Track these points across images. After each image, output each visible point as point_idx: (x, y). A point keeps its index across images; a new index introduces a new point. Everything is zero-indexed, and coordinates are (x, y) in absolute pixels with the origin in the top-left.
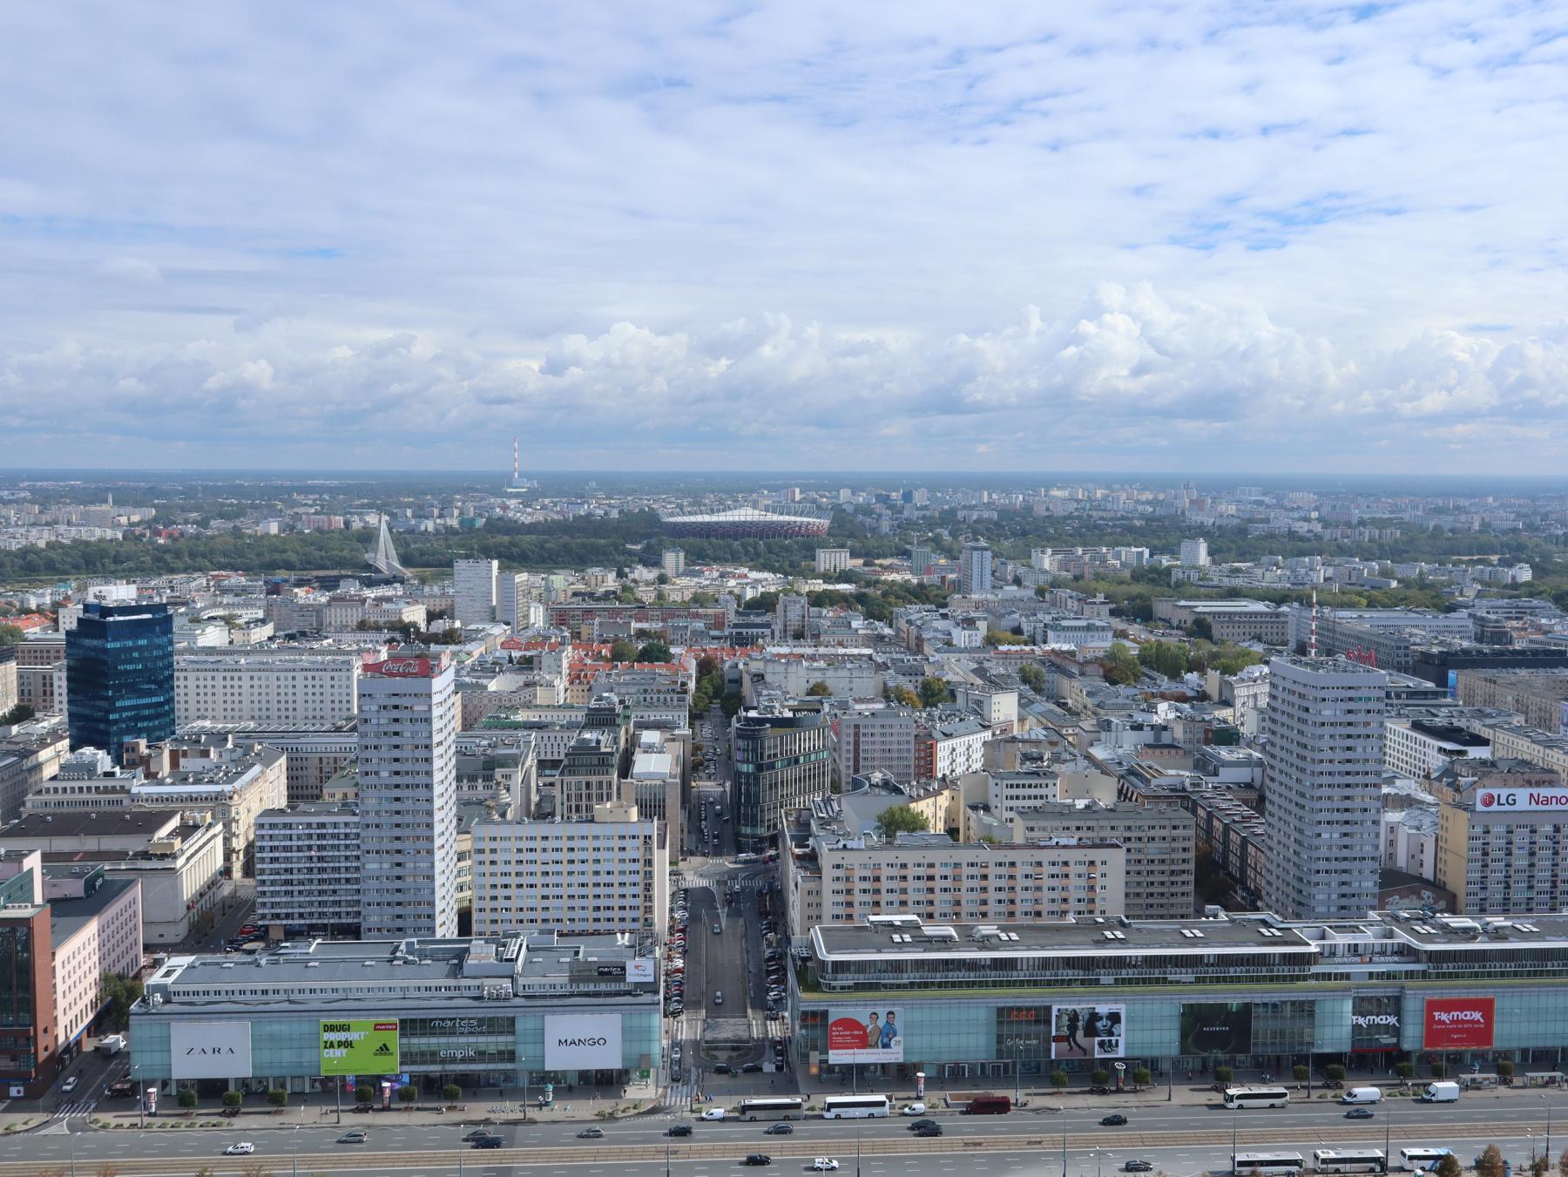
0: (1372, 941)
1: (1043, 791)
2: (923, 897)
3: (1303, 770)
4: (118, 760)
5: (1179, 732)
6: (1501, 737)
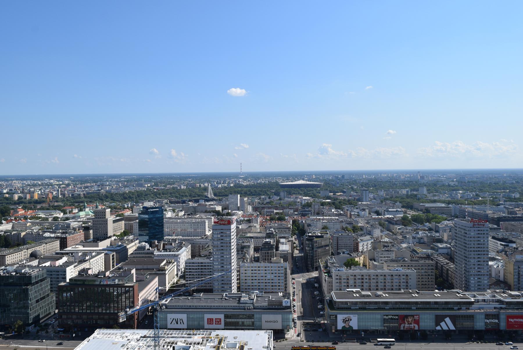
0: (489, 298)
1: (389, 256)
2: (360, 284)
3: (466, 250)
4: (150, 246)
5: (426, 239)
6: (518, 241)
